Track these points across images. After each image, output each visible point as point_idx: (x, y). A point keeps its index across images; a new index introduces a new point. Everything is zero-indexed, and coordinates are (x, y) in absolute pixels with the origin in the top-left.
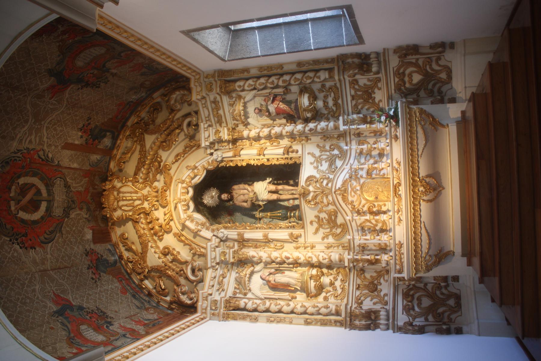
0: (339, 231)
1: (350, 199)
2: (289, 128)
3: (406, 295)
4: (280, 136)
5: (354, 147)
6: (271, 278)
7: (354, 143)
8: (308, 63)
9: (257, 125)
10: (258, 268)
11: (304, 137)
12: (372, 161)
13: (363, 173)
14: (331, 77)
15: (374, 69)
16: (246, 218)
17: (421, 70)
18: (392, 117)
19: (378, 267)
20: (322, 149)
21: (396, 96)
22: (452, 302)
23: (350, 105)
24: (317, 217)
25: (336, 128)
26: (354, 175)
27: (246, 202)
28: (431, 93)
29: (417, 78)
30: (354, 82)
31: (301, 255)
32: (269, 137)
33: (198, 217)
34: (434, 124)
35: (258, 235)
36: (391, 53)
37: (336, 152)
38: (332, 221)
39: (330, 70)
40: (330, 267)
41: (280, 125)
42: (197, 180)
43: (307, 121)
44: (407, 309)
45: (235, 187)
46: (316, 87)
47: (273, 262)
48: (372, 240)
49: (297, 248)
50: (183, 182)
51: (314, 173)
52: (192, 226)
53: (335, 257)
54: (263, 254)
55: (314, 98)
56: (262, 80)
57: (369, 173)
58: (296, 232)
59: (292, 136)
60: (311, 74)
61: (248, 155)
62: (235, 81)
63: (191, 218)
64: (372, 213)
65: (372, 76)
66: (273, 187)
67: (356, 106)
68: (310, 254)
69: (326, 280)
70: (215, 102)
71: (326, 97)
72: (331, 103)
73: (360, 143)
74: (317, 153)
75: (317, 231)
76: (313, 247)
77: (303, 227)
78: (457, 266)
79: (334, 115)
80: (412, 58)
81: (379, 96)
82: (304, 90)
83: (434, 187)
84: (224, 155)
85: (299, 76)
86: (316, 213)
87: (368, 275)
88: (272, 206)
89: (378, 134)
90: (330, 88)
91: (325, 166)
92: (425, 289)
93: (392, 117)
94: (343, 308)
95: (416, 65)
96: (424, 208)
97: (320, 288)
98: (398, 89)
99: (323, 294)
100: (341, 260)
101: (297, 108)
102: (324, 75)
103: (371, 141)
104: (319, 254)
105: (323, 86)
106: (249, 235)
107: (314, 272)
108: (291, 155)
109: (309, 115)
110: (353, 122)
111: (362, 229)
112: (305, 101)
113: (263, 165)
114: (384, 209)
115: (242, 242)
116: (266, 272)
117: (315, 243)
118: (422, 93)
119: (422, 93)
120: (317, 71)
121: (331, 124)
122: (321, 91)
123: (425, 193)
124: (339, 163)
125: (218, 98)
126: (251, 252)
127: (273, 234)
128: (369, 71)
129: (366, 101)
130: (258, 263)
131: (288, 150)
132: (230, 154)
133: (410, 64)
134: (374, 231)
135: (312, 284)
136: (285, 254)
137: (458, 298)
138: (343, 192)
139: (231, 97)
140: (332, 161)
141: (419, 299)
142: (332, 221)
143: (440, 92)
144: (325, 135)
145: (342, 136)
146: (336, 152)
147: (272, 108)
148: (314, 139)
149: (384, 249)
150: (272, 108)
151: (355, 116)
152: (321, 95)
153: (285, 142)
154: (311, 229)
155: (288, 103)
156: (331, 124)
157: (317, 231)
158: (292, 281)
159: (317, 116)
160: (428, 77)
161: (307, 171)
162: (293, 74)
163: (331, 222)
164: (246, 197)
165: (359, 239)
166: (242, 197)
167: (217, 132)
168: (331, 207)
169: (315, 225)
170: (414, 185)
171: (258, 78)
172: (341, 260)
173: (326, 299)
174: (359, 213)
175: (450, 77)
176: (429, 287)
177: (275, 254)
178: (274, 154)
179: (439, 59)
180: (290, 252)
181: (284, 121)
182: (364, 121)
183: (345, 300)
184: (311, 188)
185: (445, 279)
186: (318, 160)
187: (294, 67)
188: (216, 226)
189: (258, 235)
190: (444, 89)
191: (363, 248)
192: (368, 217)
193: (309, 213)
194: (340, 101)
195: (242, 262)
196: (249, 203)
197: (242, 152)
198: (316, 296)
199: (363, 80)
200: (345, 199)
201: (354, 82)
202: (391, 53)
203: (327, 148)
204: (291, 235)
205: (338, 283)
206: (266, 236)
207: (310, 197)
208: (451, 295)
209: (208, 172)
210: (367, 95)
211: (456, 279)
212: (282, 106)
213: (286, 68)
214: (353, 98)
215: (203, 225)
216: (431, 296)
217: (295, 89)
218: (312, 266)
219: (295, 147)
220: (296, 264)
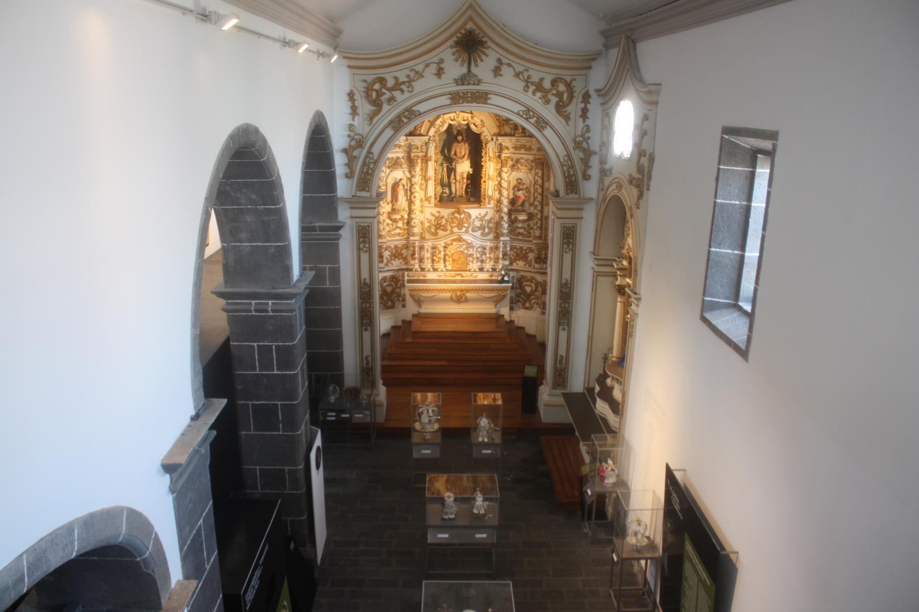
0: (433, 230)
1: (455, 243)
2: (505, 202)
3: (393, 277)
4: (500, 193)
5: (489, 244)
6: (401, 187)
7: (492, 244)
8: (547, 223)
9: (510, 177)
10: (408, 175)
11: (499, 210)
12: (478, 255)
13: (471, 252)
14: (536, 238)
15: (536, 266)
16: (442, 143)
17: (532, 292)
18: (503, 279)
19: (409, 258)
20: (489, 221)
21: (519, 275)
22: (390, 303)
23: (518, 245)
24: (443, 217)
25: (503, 235)
26: (470, 245)
27: (455, 154)
28: (518, 295)
29: (528, 289)
30: (531, 251)
31: (417, 206)
32: (500, 184)
33: (446, 126)
34: (498, 301)
35: (431, 172)
36: (544, 278)
37: (487, 230)
38: (438, 226)
39: (540, 237)
40: (408, 223)
41: (508, 195)
42: (472, 126)
43: (510, 213)
44: (384, 279)
45: (467, 145)
46: (532, 223)
47: (412, 185)
48: (428, 255)
49: (421, 200)
50: (472, 118)
51: (473, 217)
52: (438, 122)
53: (416, 230)
54: (417, 179)
55: (524, 221)
56: (540, 190)
57: (471, 255)
58: (433, 200)
59: (499, 201)
60: (539, 225)
61: (490, 168)
62: (542, 170)
63: (443, 122)
64: (445, 255)
65: (533, 263)
66: (465, 176)
67: (516, 248)
68: (417, 212)
69: (400, 224)
70: (530, 149)
71: (524, 228)
72: (521, 231)
73: (491, 249)
74: (487, 218)
75: (433, 215)
76: (422, 212)
77: (436, 206)
78: (411, 309)
79: (512, 231)
80: (540, 289)
81: (520, 264)
82: (531, 216)
83: (459, 300)
84: (490, 150)
85: (539, 216)
86: (446, 217)
87: (404, 251)
88: (451, 170)
89: (497, 260)
90: (530, 233)
91: (478, 223)
92: (396, 287)
93: (503, 279)
94: (384, 240)
95: (536, 290)
96: (448, 295)
97: (395, 221)
98: (523, 277)
99: (390, 222)
100: (413, 235)
101: (518, 211)
102: (538, 233)
103: (492, 255)
104: (417, 217)
105: (532, 228)
106: (431, 165)
107: (406, 216)
108: (487, 199)
109: (513, 217)
110: (505, 247)
111: (434, 248)
112: (522, 217)
113: (481, 178)
114: (447, 264)
115: (426, 159)
116: (404, 182)
117: (425, 212)
118: (519, 291)
119: (519, 291)
120: (541, 228)
121: (505, 231)
122: (529, 226)
123: (456, 295)
124: (478, 234)
125: (533, 152)
126: (418, 169)
127: (431, 184)
128: (536, 262)
129: (517, 255)
130: (410, 172)
131: (490, 198)
132: (491, 154)
133: (537, 287)
134: (433, 255)
135: (398, 217)
136: (417, 194)
137: (392, 307)
138: (460, 239)
139: (532, 161)
140: (482, 228)
141: (390, 285)
142: (438, 226)
143: (518, 301)
144: (498, 225)
145: (497, 237)
146: (487, 230)
147: (520, 193)
148: (497, 216)
149: (421, 260)
150: (520, 193)
151: (508, 249)
152: (526, 226)
153: (497, 196)
154: (435, 211)
155: (523, 205)
156: (505, 231)
157: (433, 215)
158: (399, 203)
159: (512, 222)
160: (528, 296)
161: (474, 212)
162: (542, 211)
163: (438, 225)
164: (459, 155)
165: (428, 245)
166: (458, 151)
167: (507, 148)
168: (449, 228)
169: (437, 215)
170: (461, 290)
171: (542, 187)
172: (413, 235)
173: (388, 224)
174: (445, 247)
175: (526, 308)
176: (398, 290)
177: (417, 187)
178: (489, 187)
179: (537, 304)
180: (419, 194)
181: (511, 196)
182: (505, 254)
183: (388, 238)
184: (463, 216)
185: (404, 300)
186: (481, 220)
187: (545, 214)
188: (437, 138)
189: (431, 172)
190: (520, 304)
191: (422, 248)
192: (442, 253)
193: (446, 212)
194: (520, 237)
195: (411, 163)
196: (454, 157)
197: (492, 164)
198: (390, 219)
199: (531, 256)
200: (454, 240)
201: (531, 251)
202: (544, 278)
203: (490, 225)
204: (431, 197)
205: (398, 231)
206: (430, 179)
207: (457, 215)
208: (393, 303)
209: (478, 136)
210: (521, 255)
211: (404, 306)
212: (520, 201)
213: (545, 208)
214: (521, 248)
215: (439, 130)
216: (393, 291)
217: (532, 209)
218: (409, 214)
219: (492, 202)
220: (410, 202)
